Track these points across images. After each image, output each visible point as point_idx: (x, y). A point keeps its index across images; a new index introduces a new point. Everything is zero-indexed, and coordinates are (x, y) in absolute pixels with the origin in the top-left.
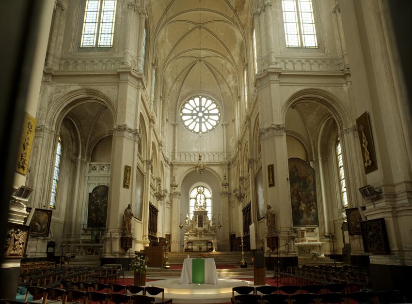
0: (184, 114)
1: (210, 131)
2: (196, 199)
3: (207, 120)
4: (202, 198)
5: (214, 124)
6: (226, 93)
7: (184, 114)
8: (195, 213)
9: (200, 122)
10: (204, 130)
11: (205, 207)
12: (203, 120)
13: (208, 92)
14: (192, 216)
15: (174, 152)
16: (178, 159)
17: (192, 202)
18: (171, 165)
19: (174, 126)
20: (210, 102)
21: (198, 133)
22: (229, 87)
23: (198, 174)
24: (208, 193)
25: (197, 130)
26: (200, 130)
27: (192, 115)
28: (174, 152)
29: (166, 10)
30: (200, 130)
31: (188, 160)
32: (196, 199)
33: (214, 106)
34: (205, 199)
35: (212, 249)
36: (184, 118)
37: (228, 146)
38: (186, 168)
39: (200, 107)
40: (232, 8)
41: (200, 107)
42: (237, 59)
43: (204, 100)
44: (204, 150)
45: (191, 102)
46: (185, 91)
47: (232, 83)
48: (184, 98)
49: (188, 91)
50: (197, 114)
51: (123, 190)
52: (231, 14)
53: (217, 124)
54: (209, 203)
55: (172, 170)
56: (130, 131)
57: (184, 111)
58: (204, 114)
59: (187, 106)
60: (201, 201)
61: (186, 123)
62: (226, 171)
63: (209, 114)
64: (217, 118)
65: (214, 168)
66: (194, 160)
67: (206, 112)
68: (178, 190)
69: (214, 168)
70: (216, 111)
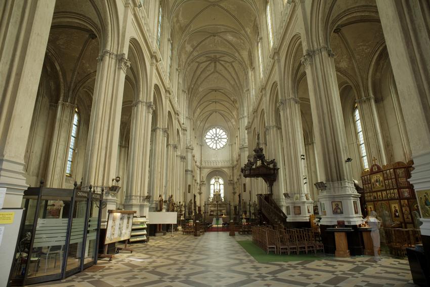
0: (207, 139)
1: (222, 148)
2: (214, 185)
3: (220, 142)
4: (217, 186)
5: (224, 144)
6: (231, 127)
7: (207, 139)
8: (214, 195)
9: (216, 143)
10: (218, 147)
11: (220, 191)
12: (218, 142)
13: (221, 126)
14: (212, 196)
15: (201, 161)
16: (204, 164)
17: (212, 187)
18: (200, 168)
19: (201, 146)
20: (222, 131)
21: (215, 149)
22: (233, 125)
23: (216, 172)
24: (221, 181)
25: (214, 147)
26: (216, 148)
27: (211, 139)
28: (201, 161)
29: (200, 101)
30: (216, 148)
31: (210, 166)
32: (214, 185)
33: (224, 133)
34: (220, 185)
35: (223, 215)
36: (207, 141)
37: (232, 157)
38: (209, 170)
39: (216, 134)
40: (231, 100)
41: (216, 134)
42: (235, 116)
43: (218, 130)
44: (219, 159)
45: (211, 131)
46: (207, 125)
47: (234, 123)
48: (207, 129)
49: (208, 125)
50: (214, 139)
51: (188, 194)
52: (232, 103)
53: (226, 144)
54: (222, 187)
55: (200, 171)
56: (190, 171)
57: (207, 137)
58: (219, 138)
59: (208, 133)
60: (217, 187)
61: (208, 144)
62: (231, 171)
63: (221, 138)
64: (226, 140)
65: (224, 169)
66: (214, 165)
67: (220, 137)
68: (205, 182)
69: (224, 169)
70: (226, 136)
